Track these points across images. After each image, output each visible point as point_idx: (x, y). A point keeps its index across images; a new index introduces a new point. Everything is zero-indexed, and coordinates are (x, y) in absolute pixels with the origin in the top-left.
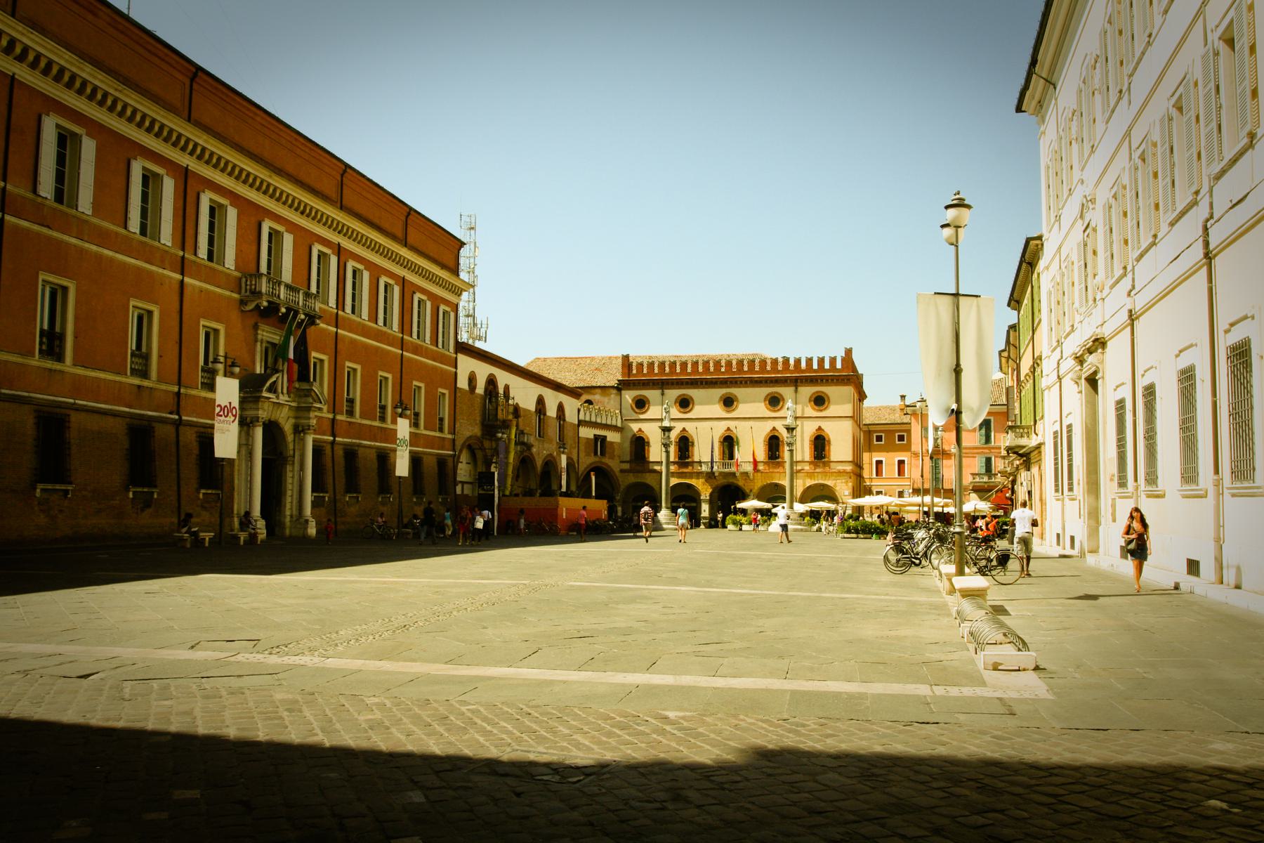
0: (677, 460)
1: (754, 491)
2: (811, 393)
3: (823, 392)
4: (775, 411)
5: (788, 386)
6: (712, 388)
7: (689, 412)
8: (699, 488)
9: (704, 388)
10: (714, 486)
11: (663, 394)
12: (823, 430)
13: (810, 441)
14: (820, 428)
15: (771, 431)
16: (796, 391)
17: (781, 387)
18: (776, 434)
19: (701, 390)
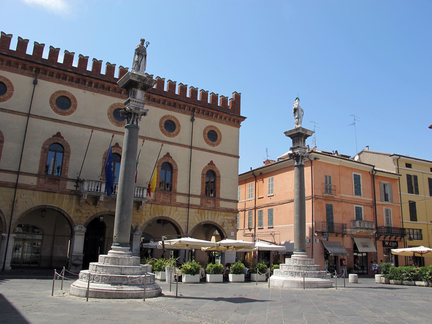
0: (43, 173)
1: (141, 225)
2: (206, 126)
3: (216, 128)
4: (169, 136)
5: (184, 113)
6: (102, 93)
7: (69, 114)
8: (71, 216)
9: (92, 90)
10: (92, 215)
11: (35, 83)
12: (215, 166)
13: (203, 174)
14: (211, 163)
15: (165, 156)
16: (192, 120)
17: (178, 112)
18: (170, 161)
19: (86, 92)
